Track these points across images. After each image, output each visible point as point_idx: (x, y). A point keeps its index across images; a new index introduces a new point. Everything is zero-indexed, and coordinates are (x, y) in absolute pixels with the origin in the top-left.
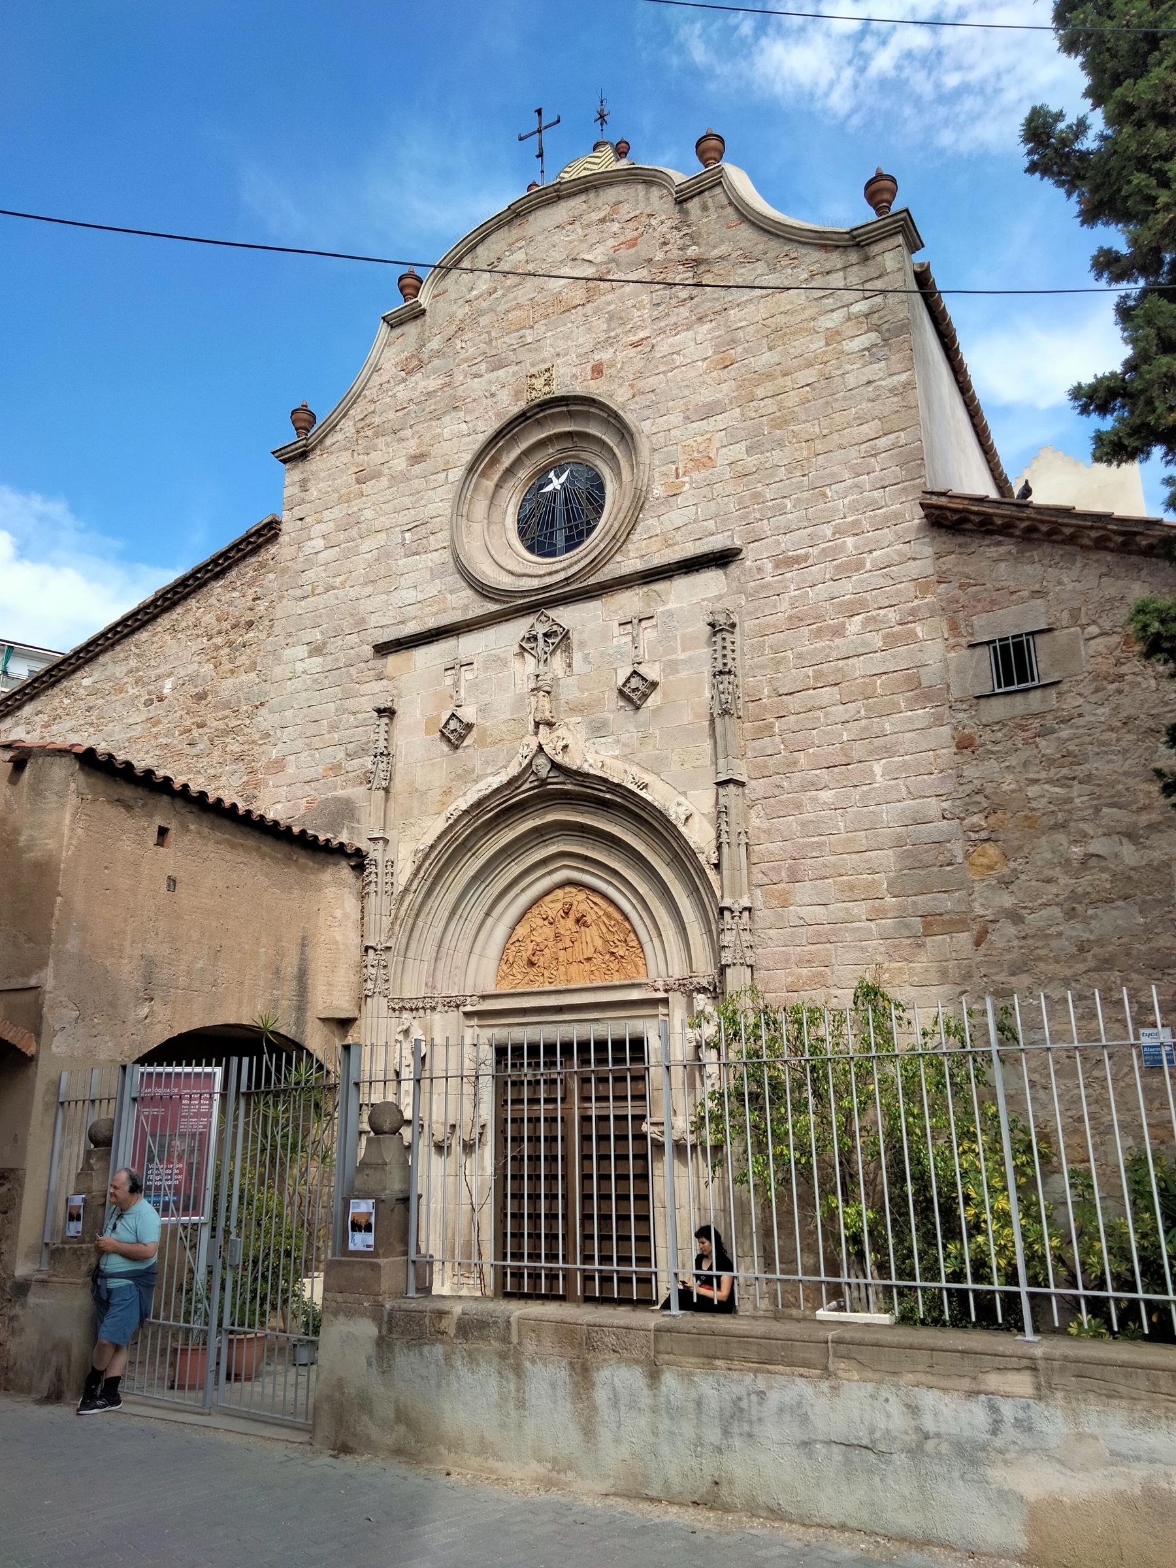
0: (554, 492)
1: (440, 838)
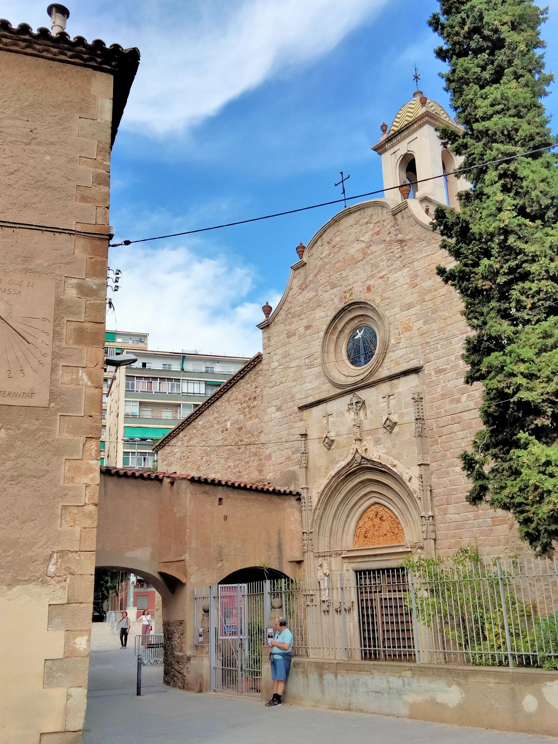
0: (359, 339)
1: (325, 487)
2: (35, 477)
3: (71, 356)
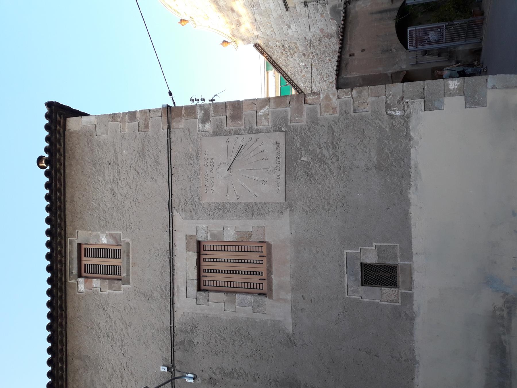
2: (333, 134)
3: (250, 122)
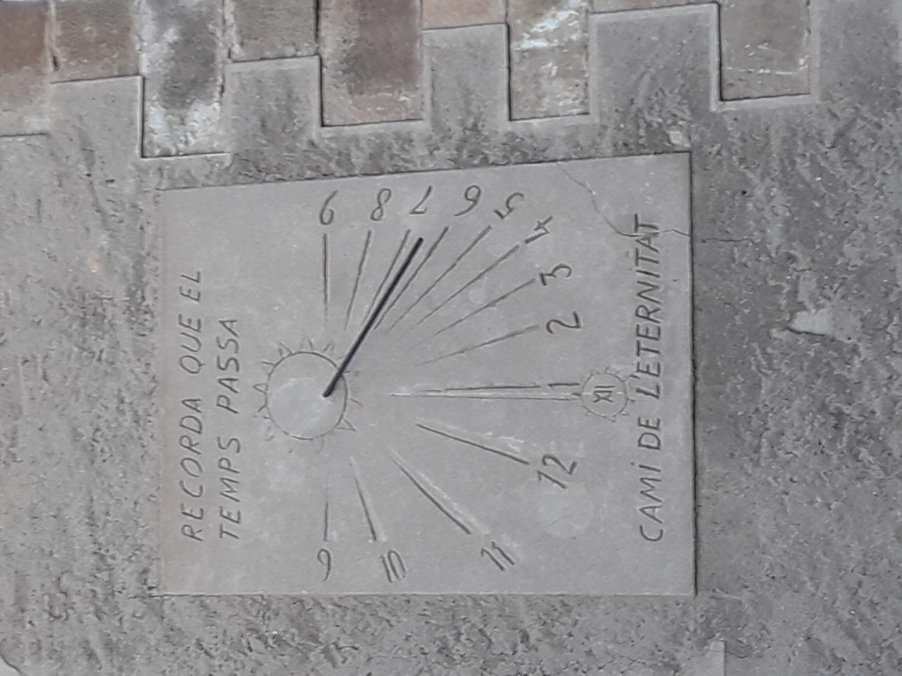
3: (467, 93)
